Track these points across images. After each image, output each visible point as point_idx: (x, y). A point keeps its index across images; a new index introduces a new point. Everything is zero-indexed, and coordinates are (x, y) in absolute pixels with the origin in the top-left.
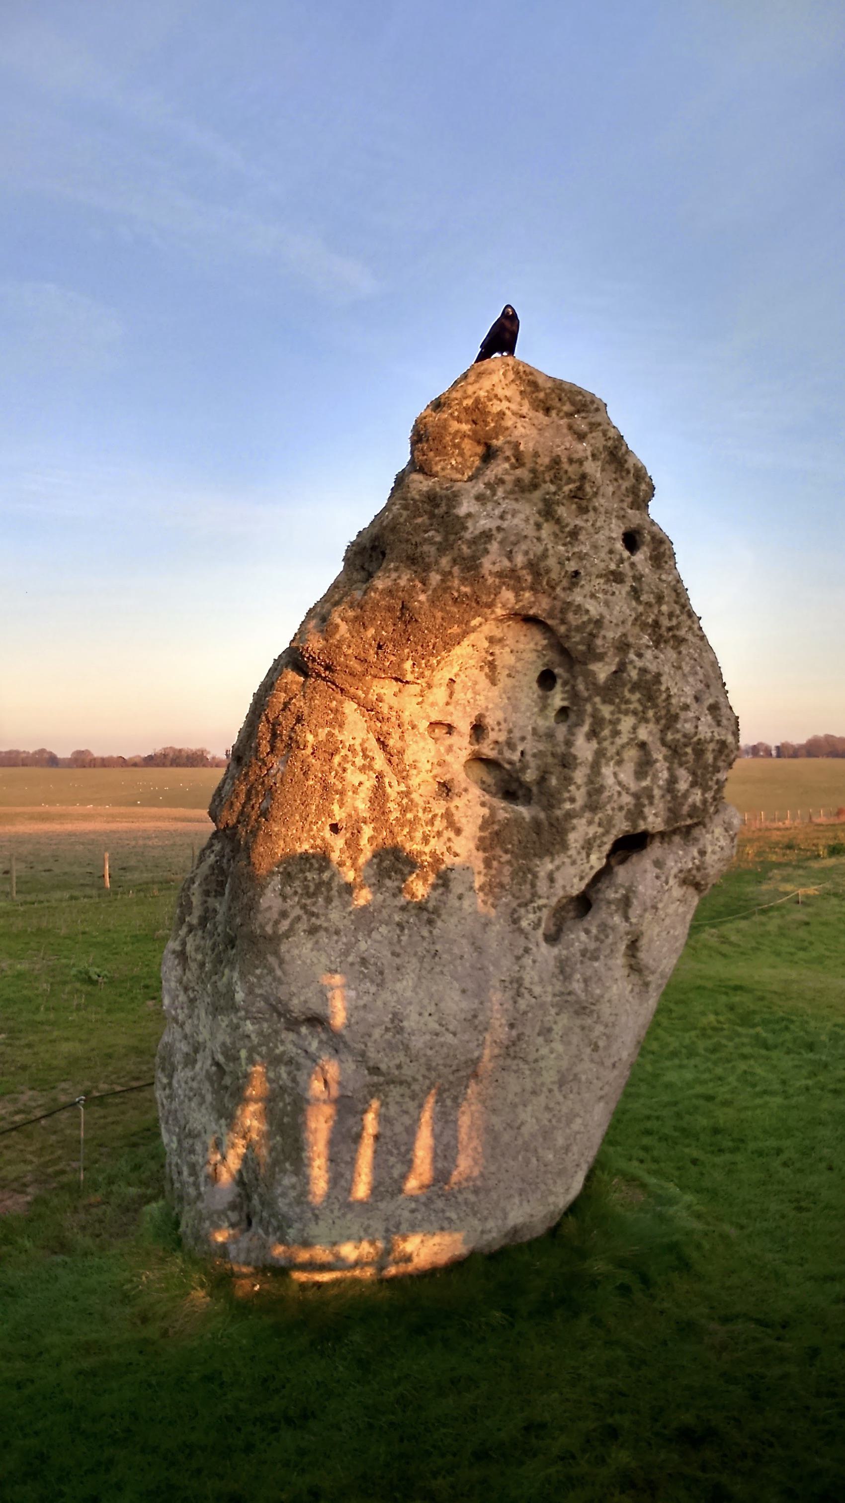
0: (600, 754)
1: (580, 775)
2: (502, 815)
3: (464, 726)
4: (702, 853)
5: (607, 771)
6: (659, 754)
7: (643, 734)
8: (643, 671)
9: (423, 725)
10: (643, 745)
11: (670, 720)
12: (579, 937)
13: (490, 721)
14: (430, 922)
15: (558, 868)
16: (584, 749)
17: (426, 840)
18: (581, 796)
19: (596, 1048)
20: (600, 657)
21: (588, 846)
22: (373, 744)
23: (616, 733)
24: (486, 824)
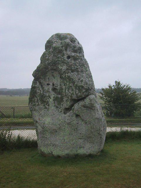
0: (66, 87)
1: (64, 91)
2: (56, 96)
3: (51, 84)
4: (85, 103)
5: (67, 91)
6: (74, 88)
7: (70, 85)
8: (68, 76)
9: (46, 84)
10: (71, 86)
11: (74, 83)
12: (68, 114)
13: (55, 83)
14: (48, 110)
15: (63, 104)
16: (64, 87)
17: (46, 99)
18: (64, 94)
19: (74, 130)
20: (63, 74)
21: (67, 101)
22: (40, 87)
23: (67, 85)
24: (54, 97)
